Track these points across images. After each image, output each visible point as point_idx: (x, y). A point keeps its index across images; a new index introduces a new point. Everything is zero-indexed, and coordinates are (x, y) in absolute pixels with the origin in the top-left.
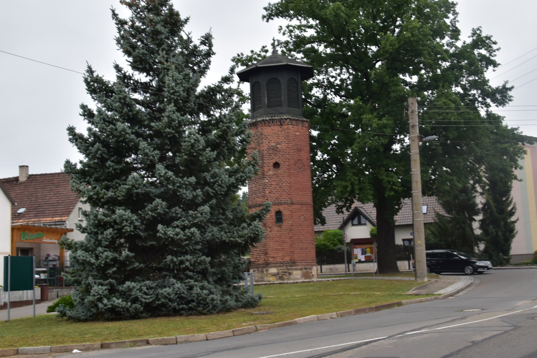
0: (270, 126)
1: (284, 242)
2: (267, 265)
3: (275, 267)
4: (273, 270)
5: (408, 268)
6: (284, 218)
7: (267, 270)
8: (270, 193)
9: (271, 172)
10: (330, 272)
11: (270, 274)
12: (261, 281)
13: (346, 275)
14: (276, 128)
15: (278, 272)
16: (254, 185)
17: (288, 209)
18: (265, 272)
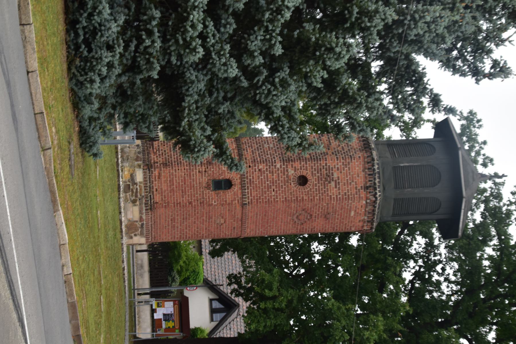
0: (363, 171)
2: (148, 166)
3: (145, 178)
4: (139, 176)
6: (221, 192)
7: (139, 166)
9: (293, 172)
10: (137, 264)
11: (134, 171)
13: (132, 290)
14: (360, 180)
15: (136, 184)
18: (136, 163)
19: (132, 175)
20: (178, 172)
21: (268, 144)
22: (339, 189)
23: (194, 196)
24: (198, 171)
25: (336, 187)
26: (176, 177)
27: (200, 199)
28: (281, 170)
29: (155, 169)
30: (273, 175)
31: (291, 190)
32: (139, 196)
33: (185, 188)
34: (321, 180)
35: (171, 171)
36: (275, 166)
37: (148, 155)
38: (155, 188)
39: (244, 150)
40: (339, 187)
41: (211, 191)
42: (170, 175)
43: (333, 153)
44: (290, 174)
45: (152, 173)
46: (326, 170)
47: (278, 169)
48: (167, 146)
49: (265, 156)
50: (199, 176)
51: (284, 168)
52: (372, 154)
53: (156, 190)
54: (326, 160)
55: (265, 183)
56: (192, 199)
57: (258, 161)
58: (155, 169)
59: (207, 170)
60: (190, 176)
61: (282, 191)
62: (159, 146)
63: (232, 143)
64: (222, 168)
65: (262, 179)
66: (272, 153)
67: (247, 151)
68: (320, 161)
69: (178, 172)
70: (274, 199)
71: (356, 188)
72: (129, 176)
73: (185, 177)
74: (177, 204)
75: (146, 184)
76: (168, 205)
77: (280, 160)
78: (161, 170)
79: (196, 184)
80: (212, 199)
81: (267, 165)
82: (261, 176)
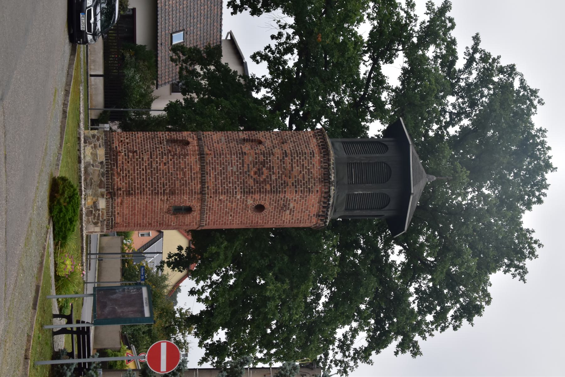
0: (318, 203)
1: (144, 216)
2: (111, 194)
3: (107, 206)
4: (102, 204)
7: (102, 196)
8: (220, 200)
9: (252, 202)
12: (85, 180)
13: (88, 76)
15: (99, 210)
16: (235, 170)
17: (193, 222)
18: (100, 190)
19: (94, 203)
20: (141, 201)
21: (232, 166)
22: (293, 215)
23: (154, 219)
25: (290, 214)
26: (138, 204)
29: (118, 197)
30: (232, 204)
31: (247, 215)
32: (101, 219)
33: (146, 213)
34: (278, 208)
36: (235, 197)
37: (112, 179)
38: (116, 212)
39: (207, 174)
42: (132, 203)
43: (293, 185)
44: (248, 203)
45: (115, 200)
46: (284, 201)
47: (238, 199)
48: (131, 164)
49: (227, 185)
51: (244, 199)
52: (329, 191)
53: (118, 213)
55: (223, 210)
56: (151, 221)
57: (219, 192)
58: (118, 197)
61: (239, 216)
62: (123, 164)
63: (196, 161)
65: (221, 207)
66: (234, 180)
67: (210, 177)
68: (279, 194)
69: (141, 201)
70: (230, 222)
71: (309, 215)
72: (92, 203)
73: (146, 205)
74: (137, 224)
76: (129, 225)
77: (241, 192)
79: (158, 209)
80: (171, 221)
81: (227, 196)
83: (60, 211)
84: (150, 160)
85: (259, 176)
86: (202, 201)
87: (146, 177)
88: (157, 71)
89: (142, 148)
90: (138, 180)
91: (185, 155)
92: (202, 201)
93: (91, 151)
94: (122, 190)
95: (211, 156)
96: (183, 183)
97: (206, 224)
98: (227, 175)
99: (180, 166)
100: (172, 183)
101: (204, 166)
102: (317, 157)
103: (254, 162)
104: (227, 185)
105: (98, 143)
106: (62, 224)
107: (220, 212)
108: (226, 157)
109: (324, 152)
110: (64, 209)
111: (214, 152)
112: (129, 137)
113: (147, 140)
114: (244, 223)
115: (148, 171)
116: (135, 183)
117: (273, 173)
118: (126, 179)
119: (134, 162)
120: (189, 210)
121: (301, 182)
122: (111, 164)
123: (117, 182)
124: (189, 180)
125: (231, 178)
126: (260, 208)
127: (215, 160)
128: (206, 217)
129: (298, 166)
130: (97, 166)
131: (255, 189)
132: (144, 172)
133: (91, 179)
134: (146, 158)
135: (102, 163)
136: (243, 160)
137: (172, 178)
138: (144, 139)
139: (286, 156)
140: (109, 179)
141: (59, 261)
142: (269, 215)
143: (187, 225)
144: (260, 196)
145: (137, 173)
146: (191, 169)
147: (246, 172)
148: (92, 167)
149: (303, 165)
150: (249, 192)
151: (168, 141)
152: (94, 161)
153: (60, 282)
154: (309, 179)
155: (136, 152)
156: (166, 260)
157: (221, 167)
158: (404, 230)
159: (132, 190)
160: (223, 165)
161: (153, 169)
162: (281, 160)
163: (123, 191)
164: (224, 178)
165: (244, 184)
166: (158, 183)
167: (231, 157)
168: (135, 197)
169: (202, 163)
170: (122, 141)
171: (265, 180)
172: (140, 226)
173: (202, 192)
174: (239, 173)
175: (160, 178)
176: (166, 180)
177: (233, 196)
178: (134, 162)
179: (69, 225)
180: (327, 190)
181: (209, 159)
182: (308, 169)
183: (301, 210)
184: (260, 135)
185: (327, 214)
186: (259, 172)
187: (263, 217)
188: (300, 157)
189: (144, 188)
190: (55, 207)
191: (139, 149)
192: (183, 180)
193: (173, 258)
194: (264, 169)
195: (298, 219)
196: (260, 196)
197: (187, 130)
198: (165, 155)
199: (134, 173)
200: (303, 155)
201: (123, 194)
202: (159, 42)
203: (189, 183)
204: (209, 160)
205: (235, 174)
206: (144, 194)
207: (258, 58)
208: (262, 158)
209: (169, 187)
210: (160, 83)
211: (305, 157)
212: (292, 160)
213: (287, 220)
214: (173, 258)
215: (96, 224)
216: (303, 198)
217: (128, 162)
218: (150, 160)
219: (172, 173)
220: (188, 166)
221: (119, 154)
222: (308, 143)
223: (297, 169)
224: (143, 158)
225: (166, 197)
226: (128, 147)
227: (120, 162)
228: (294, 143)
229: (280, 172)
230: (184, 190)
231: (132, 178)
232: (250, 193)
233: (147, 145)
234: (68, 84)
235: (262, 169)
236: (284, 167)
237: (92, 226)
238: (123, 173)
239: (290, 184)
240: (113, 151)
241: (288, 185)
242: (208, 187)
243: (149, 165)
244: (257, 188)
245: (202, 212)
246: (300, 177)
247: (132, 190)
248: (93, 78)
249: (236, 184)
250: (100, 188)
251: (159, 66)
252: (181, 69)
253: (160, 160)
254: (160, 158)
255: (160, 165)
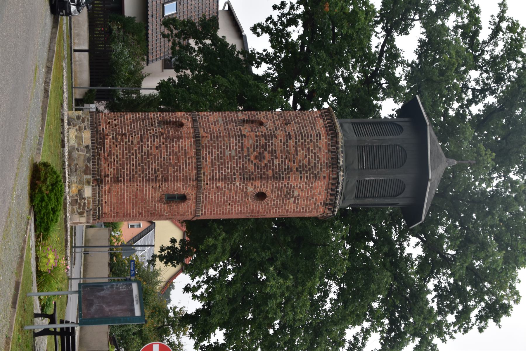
0: (325, 190)
1: (135, 205)
2: (98, 181)
3: (94, 194)
4: (88, 192)
5: (76, 48)
7: (88, 183)
8: (217, 187)
9: (252, 189)
12: (69, 165)
13: (71, 51)
15: (84, 199)
16: (233, 154)
18: (86, 177)
19: (79, 191)
21: (230, 150)
22: (298, 204)
24: (151, 187)
25: (294, 202)
26: (127, 192)
27: (152, 211)
28: (240, 188)
30: (231, 192)
33: (136, 202)
34: (281, 196)
35: (123, 187)
36: (234, 184)
38: (104, 201)
39: (203, 159)
40: (298, 203)
41: (164, 204)
42: (121, 191)
43: (297, 171)
44: (248, 191)
45: (102, 188)
46: (287, 188)
47: (237, 187)
49: (225, 170)
50: (152, 191)
53: (105, 202)
54: (289, 180)
55: (221, 198)
56: (142, 210)
57: (216, 179)
59: (161, 186)
60: (143, 191)
62: (110, 148)
63: (191, 145)
64: (177, 185)
65: (218, 195)
66: (233, 165)
67: (206, 162)
68: (283, 180)
70: (229, 211)
71: (315, 204)
72: (77, 191)
73: (137, 193)
74: (127, 214)
75: (95, 199)
76: (117, 215)
77: (241, 179)
78: (112, 186)
79: (149, 198)
80: (164, 211)
81: (225, 183)
82: (218, 192)
83: (42, 200)
84: (141, 143)
85: (260, 161)
86: (198, 188)
87: (136, 162)
88: (147, 46)
89: (131, 131)
90: (127, 165)
91: (179, 138)
92: (198, 188)
93: (76, 133)
94: (110, 176)
95: (207, 139)
96: (177, 169)
97: (202, 214)
98: (224, 160)
99: (173, 151)
100: (164, 169)
101: (200, 150)
102: (324, 140)
103: (254, 145)
104: (225, 170)
105: (83, 125)
106: (44, 214)
107: (218, 200)
108: (224, 140)
109: (331, 134)
110: (46, 198)
111: (211, 134)
112: (118, 119)
113: (137, 122)
114: (244, 213)
115: (139, 156)
116: (124, 169)
117: (276, 158)
118: (114, 164)
119: (123, 146)
120: (183, 198)
121: (306, 167)
122: (97, 148)
123: (105, 168)
124: (183, 165)
125: (230, 163)
126: (261, 196)
127: (212, 144)
128: (202, 206)
129: (303, 150)
130: (82, 151)
131: (256, 175)
132: (134, 157)
133: (76, 165)
134: (135, 141)
135: (87, 147)
136: (242, 143)
137: (164, 165)
138: (133, 120)
139: (290, 139)
140: (95, 165)
141: (41, 254)
142: (271, 203)
143: (181, 215)
144: (261, 182)
145: (127, 158)
146: (185, 153)
147: (246, 156)
148: (77, 152)
149: (309, 148)
150: (249, 179)
151: (159, 123)
152: (79, 144)
153: (42, 278)
154: (315, 164)
155: (125, 134)
156: (158, 254)
157: (218, 151)
158: (421, 220)
159: (121, 177)
160: (221, 148)
161: (143, 154)
162: (284, 144)
163: (111, 178)
164: (221, 163)
165: (243, 170)
166: (149, 168)
167: (229, 140)
168: (124, 184)
169: (197, 146)
170: (109, 123)
171: (266, 165)
172: (130, 216)
173: (198, 179)
174: (238, 158)
175: (152, 163)
176: (158, 166)
177: (231, 183)
178: (123, 146)
179: (51, 215)
180: (335, 176)
181: (205, 142)
182: (315, 153)
183: (307, 198)
184: (261, 115)
185: (335, 203)
186: (260, 157)
187: (265, 206)
188: (305, 140)
189: (133, 175)
190: (36, 195)
191: (128, 132)
192: (177, 166)
193: (166, 252)
194: (266, 153)
195: (303, 208)
196: (261, 182)
197: (181, 111)
198: (157, 138)
199: (123, 158)
200: (308, 138)
201: (111, 181)
202: (150, 13)
203: (183, 168)
204: (206, 144)
205: (234, 159)
206: (133, 181)
207: (259, 30)
208: (263, 141)
209: (162, 173)
210: (150, 59)
211: (311, 140)
212: (296, 142)
213: (291, 209)
214: (166, 252)
215: (81, 214)
216: (309, 185)
217: (116, 146)
218: (141, 143)
219: (164, 158)
220: (182, 149)
221: (106, 137)
222: (314, 124)
223: (302, 153)
224: (132, 142)
225: (158, 184)
226: (116, 129)
227: (107, 146)
228: (299, 124)
229: (284, 157)
230: (177, 177)
231: (120, 164)
232: (250, 179)
233: (137, 128)
234: (50, 60)
235: (263, 153)
236: (287, 150)
237: (77, 216)
238: (111, 158)
239: (294, 169)
240: (100, 134)
241: (292, 171)
242: (204, 173)
243: (139, 149)
244: (258, 174)
245: (197, 201)
246: (305, 162)
247: (121, 177)
248: (77, 53)
249: (234, 169)
250: (86, 174)
251: (150, 39)
252: (174, 44)
253: (151, 144)
254: (151, 141)
255: (151, 149)
